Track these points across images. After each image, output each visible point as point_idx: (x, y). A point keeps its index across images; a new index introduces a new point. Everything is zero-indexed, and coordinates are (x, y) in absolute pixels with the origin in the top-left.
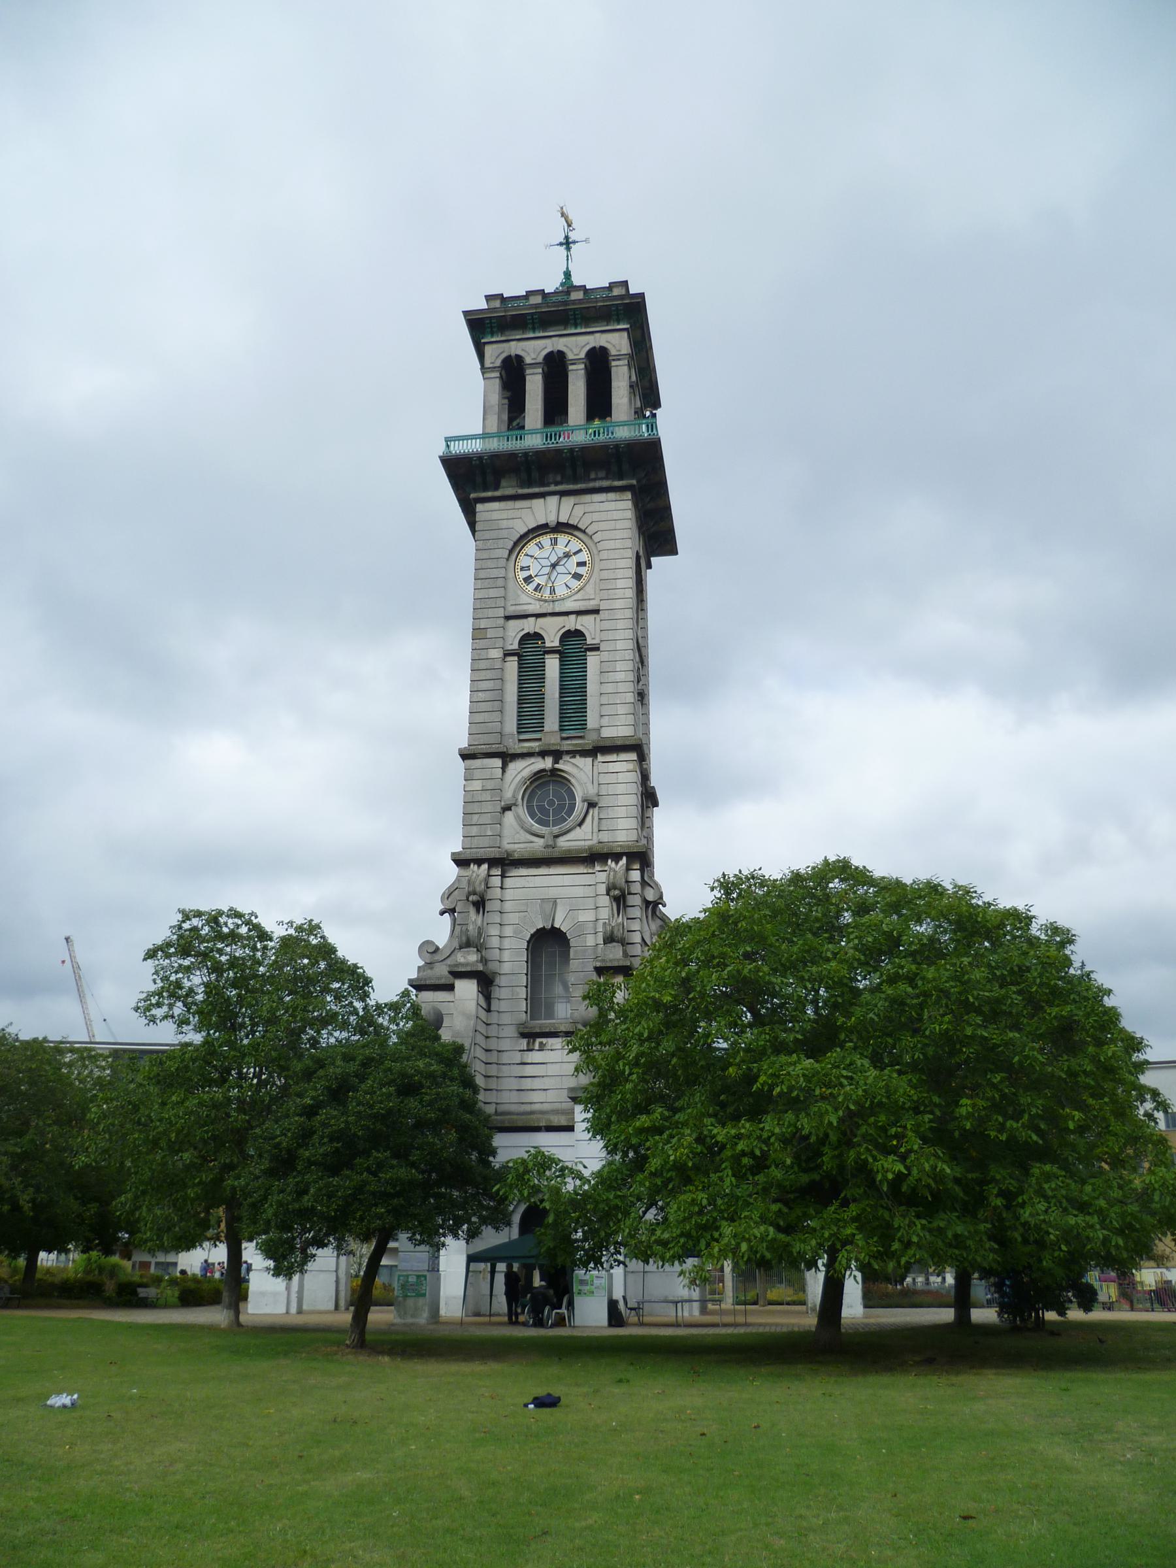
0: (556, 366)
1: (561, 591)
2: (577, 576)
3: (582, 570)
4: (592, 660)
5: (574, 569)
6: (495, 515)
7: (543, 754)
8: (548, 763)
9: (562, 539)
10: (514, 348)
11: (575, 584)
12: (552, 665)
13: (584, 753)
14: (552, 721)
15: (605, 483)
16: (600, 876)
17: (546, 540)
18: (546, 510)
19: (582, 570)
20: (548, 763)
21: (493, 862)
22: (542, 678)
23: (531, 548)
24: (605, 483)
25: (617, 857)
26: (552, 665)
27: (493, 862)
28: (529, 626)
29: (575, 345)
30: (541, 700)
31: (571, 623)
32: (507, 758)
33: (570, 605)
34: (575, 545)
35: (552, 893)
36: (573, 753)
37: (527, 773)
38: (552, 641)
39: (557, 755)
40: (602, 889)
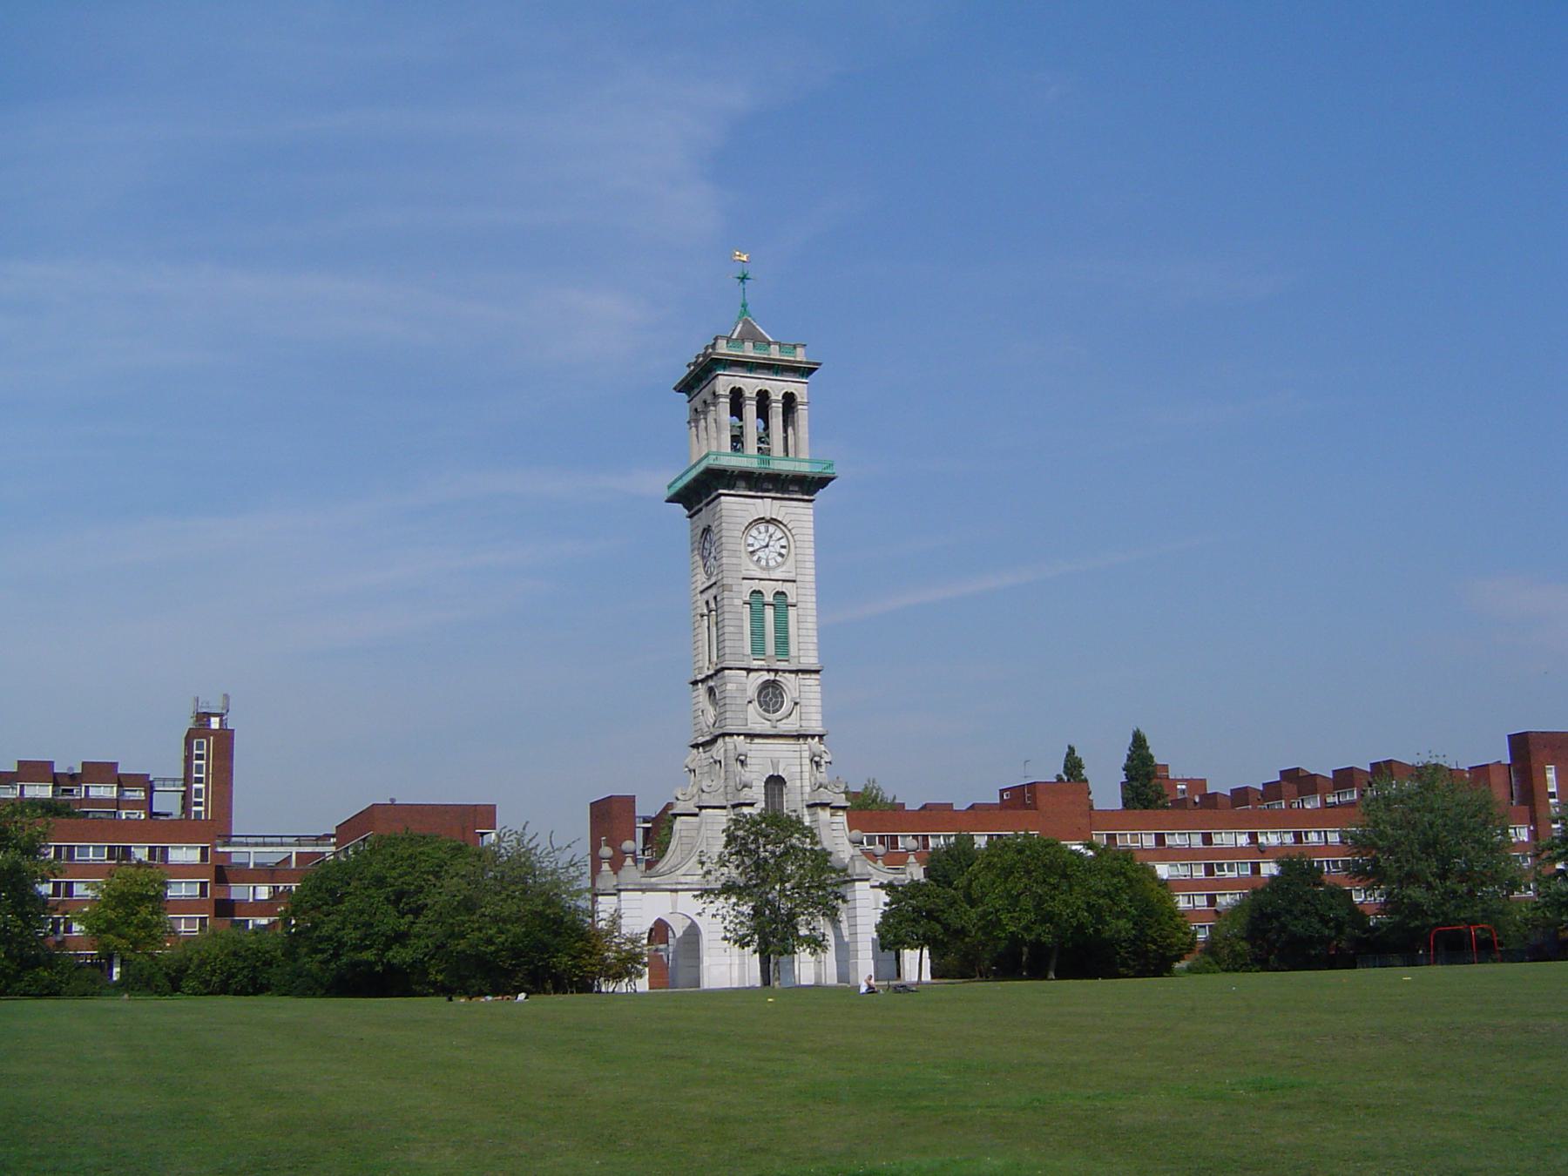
0: (763, 397)
1: (772, 563)
2: (781, 555)
3: (783, 551)
4: (792, 612)
5: (778, 549)
6: (735, 507)
7: (769, 671)
8: (771, 676)
9: (772, 528)
10: (739, 382)
11: (779, 559)
12: (769, 612)
13: (791, 672)
14: (770, 648)
15: (799, 496)
16: (805, 748)
17: (762, 527)
18: (766, 506)
19: (783, 551)
20: (771, 676)
21: (746, 735)
22: (762, 620)
23: (754, 532)
24: (799, 496)
25: (813, 736)
26: (769, 612)
27: (746, 735)
28: (756, 585)
29: (777, 387)
30: (763, 635)
31: (780, 587)
32: (749, 670)
33: (777, 574)
34: (779, 534)
35: (777, 755)
36: (784, 671)
37: (760, 681)
38: (769, 598)
39: (776, 671)
40: (806, 754)
